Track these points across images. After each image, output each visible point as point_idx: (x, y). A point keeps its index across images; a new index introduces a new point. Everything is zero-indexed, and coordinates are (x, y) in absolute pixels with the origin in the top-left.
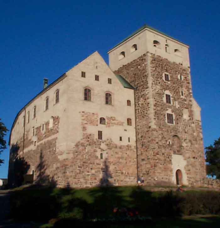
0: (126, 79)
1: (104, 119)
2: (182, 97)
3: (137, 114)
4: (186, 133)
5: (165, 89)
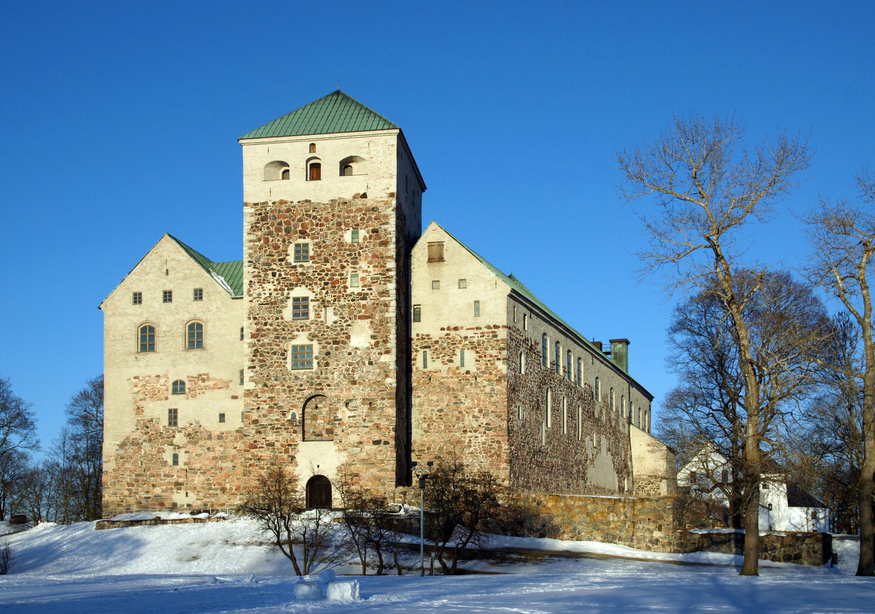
1: (182, 383)
2: (349, 291)
4: (354, 382)
5: (291, 287)
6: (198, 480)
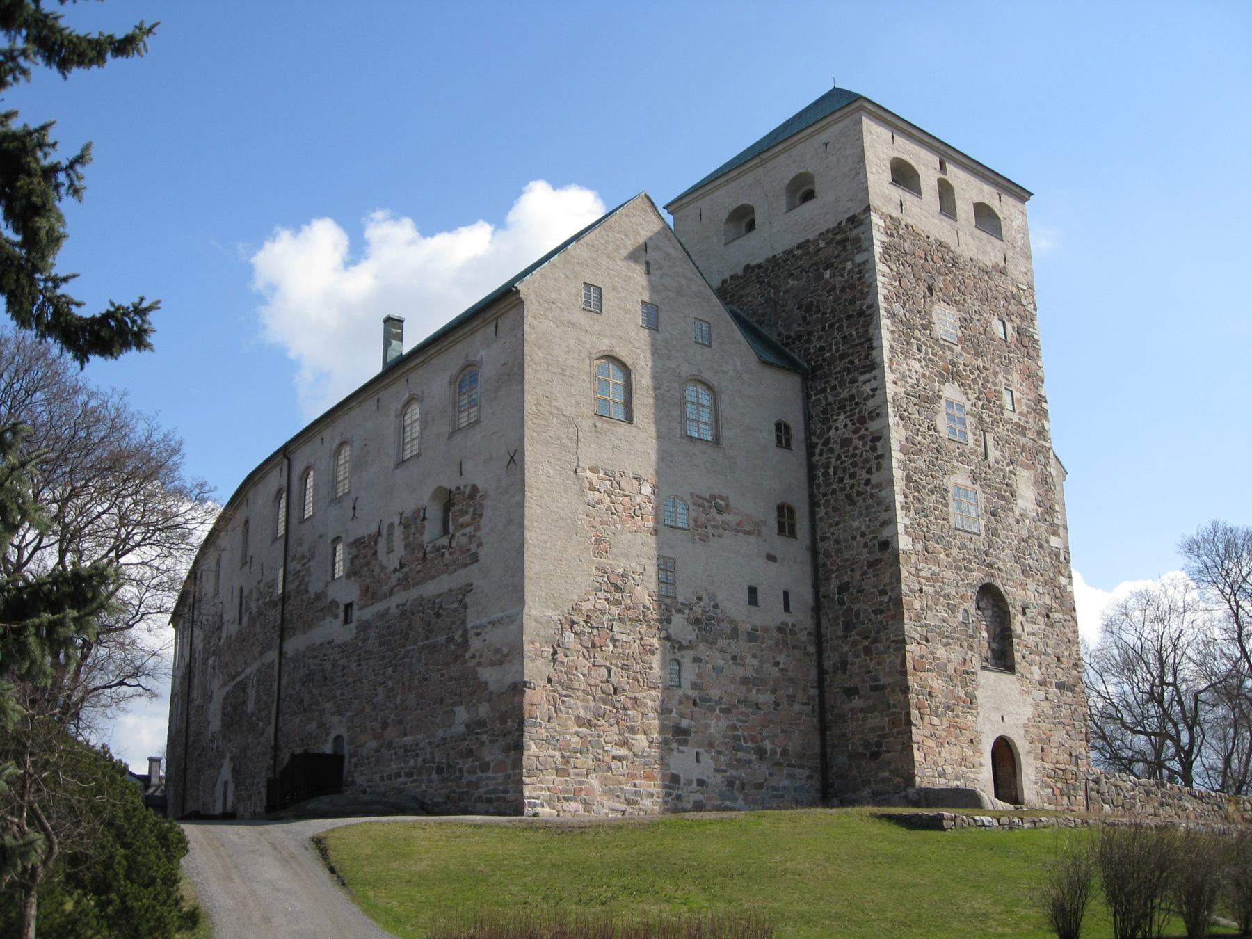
0: (764, 331)
2: (1007, 415)
3: (819, 486)
6: (717, 725)
